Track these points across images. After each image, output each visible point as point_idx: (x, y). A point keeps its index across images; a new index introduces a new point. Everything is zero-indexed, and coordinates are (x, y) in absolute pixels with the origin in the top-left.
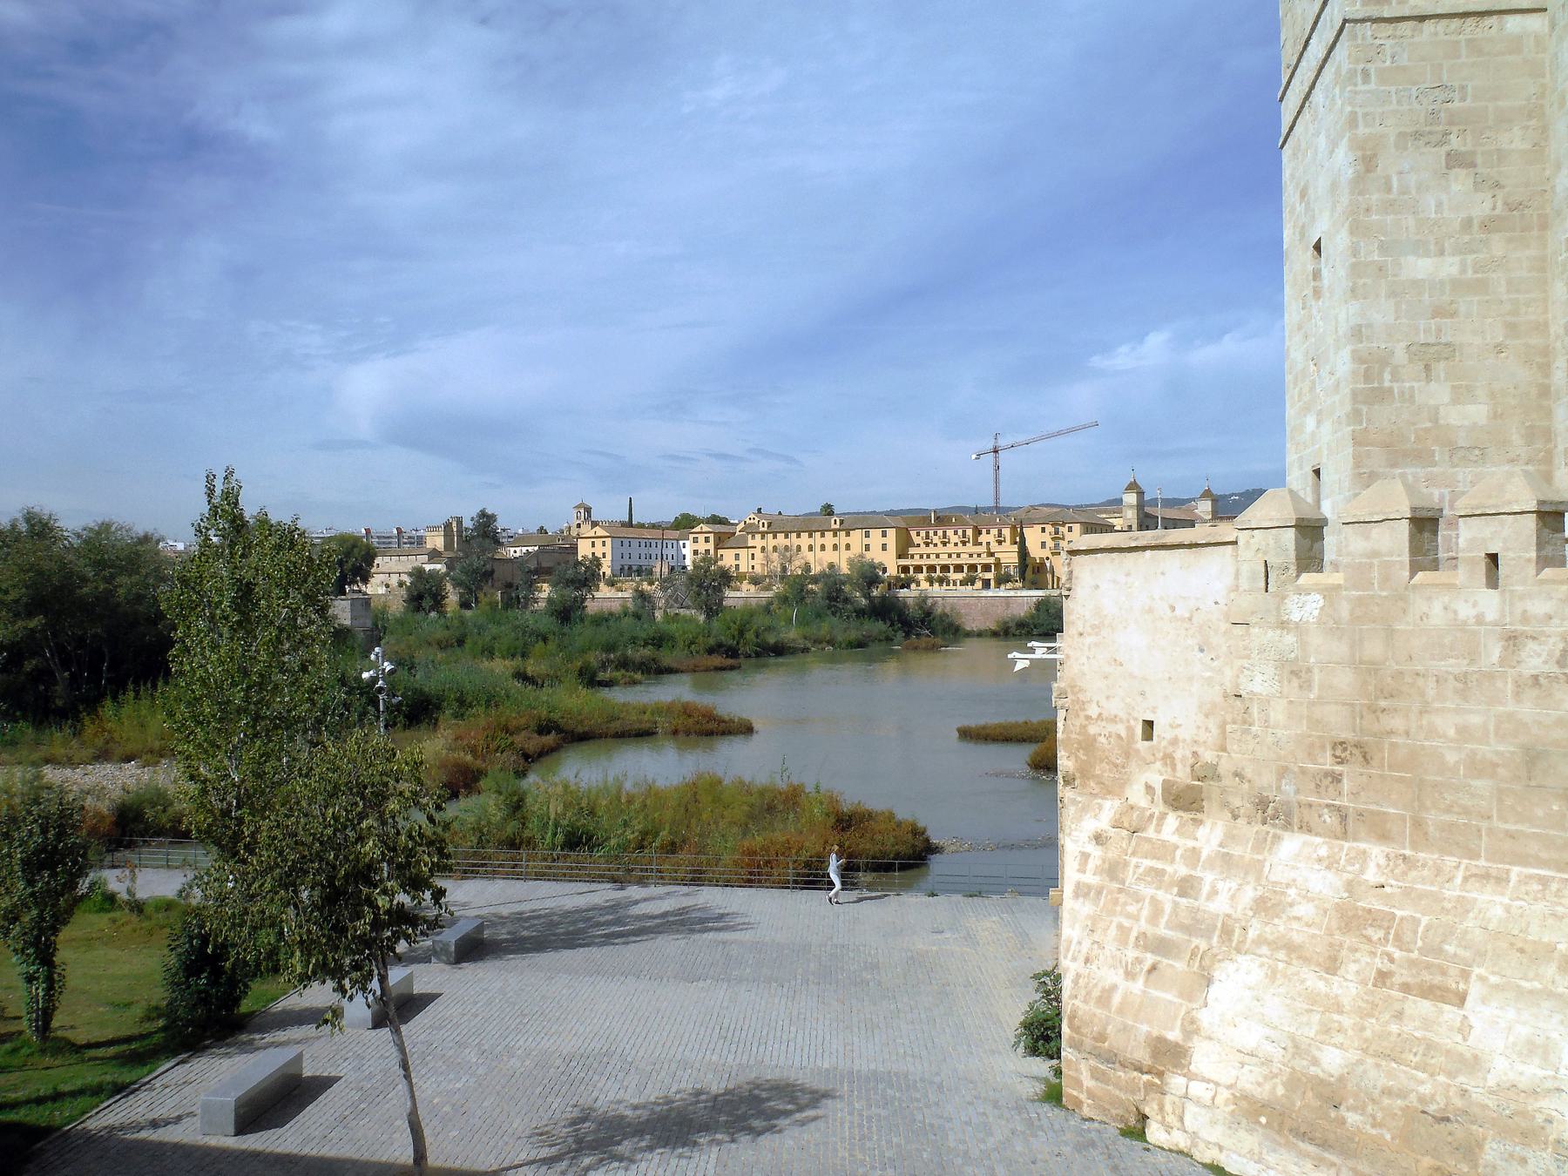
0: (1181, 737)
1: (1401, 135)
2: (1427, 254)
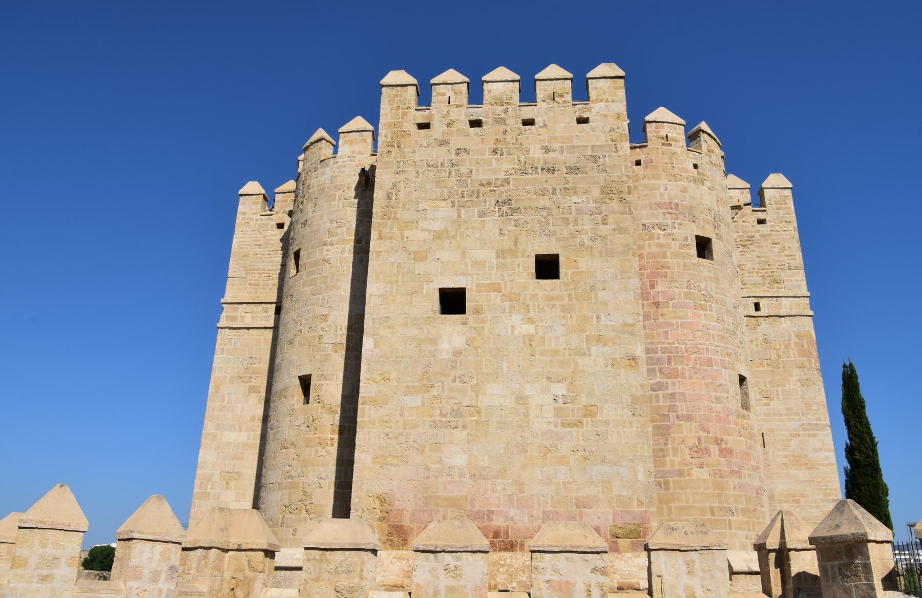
1: (232, 377)
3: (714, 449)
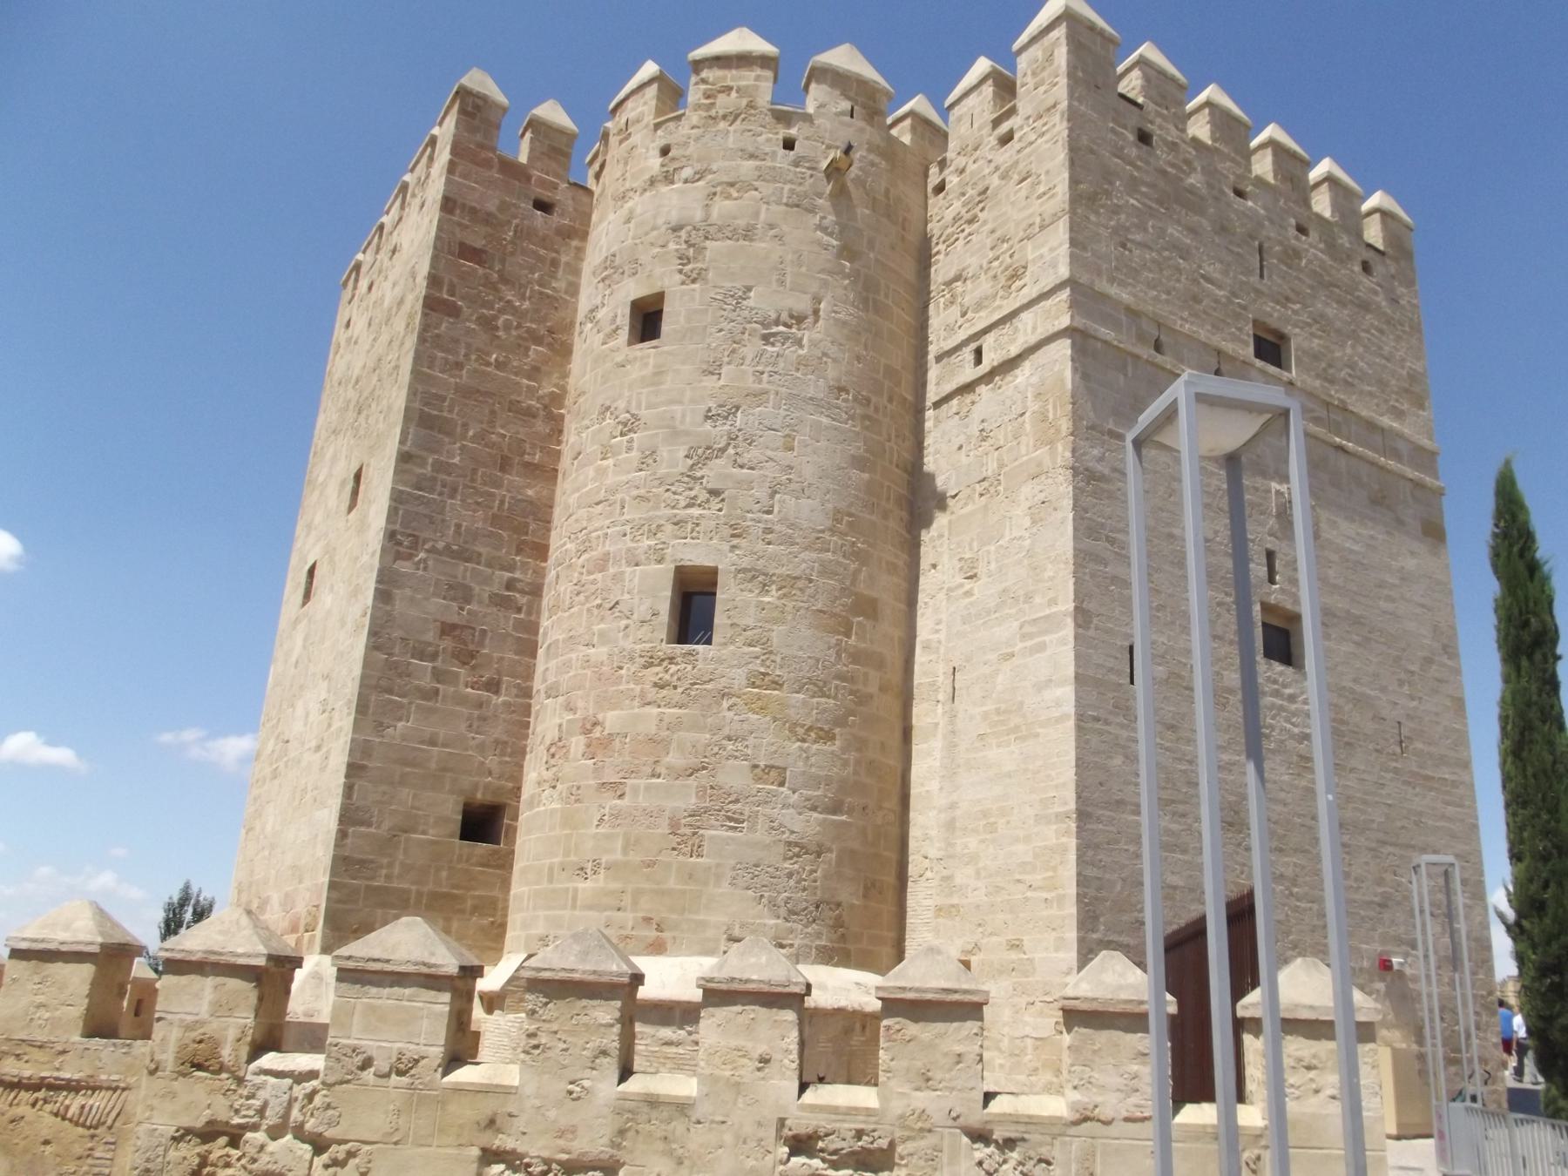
3: (577, 743)
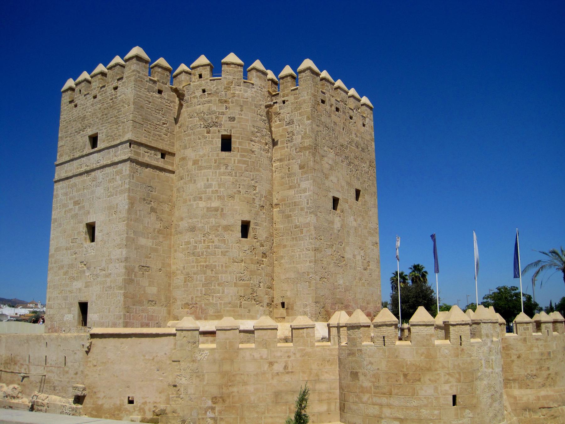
0: (148, 401)
1: (140, 198)
2: (144, 237)
